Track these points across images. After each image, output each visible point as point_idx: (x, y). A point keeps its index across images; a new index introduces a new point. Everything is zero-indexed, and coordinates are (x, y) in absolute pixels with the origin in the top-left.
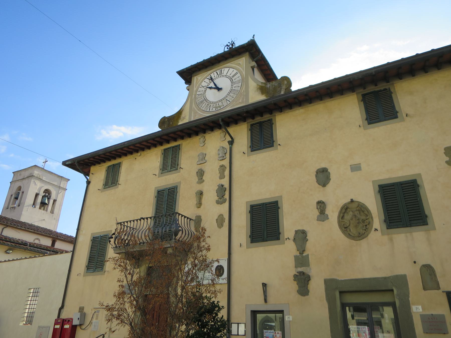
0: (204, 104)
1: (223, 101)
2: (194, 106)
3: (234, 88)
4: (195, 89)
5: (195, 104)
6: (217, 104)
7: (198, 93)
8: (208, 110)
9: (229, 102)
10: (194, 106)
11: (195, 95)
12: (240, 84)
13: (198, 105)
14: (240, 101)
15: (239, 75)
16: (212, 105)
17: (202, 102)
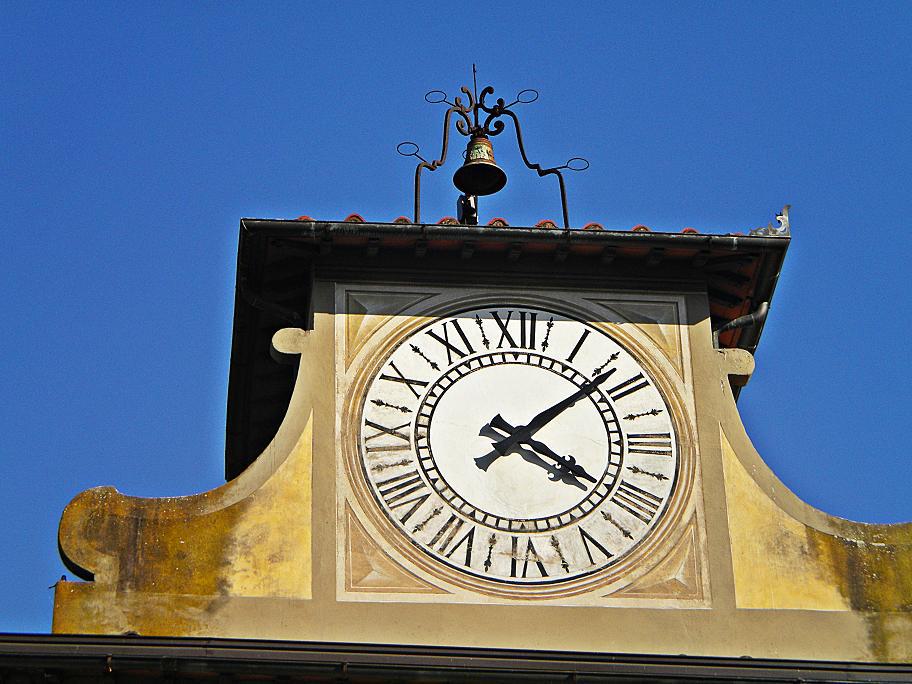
0: (425, 509)
1: (560, 534)
2: (343, 490)
3: (626, 475)
4: (345, 377)
5: (352, 480)
6: (523, 539)
7: (370, 412)
8: (458, 558)
9: (600, 559)
10: (343, 490)
11: (355, 420)
12: (668, 466)
13: (379, 498)
14: (679, 574)
15: (649, 397)
16: (482, 535)
17: (408, 485)
